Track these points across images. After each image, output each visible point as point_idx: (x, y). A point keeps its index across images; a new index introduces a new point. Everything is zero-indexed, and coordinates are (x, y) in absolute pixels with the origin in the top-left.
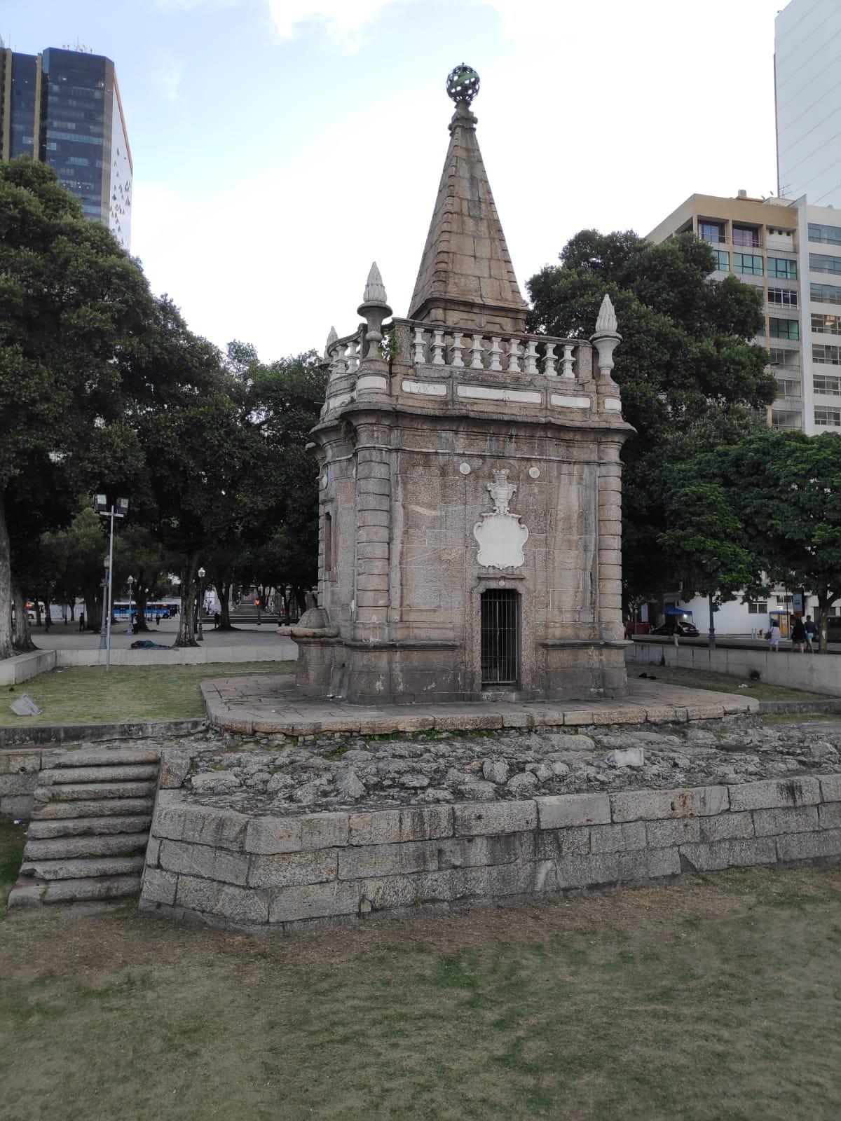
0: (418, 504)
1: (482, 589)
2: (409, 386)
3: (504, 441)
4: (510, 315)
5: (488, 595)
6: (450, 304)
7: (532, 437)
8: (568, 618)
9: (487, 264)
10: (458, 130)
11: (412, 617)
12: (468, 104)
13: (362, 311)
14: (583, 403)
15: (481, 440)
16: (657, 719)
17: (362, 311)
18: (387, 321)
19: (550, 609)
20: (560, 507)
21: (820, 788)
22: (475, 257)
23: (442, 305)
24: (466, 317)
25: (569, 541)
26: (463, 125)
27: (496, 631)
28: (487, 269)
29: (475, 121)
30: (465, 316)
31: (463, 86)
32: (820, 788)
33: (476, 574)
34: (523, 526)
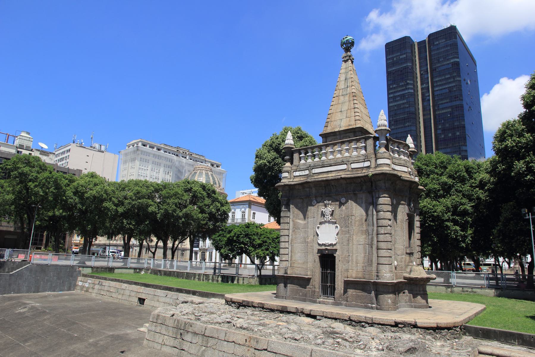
8: (360, 268)
11: (295, 265)
14: (367, 164)
16: (356, 319)
19: (350, 263)
20: (357, 215)
21: (311, 353)
32: (311, 353)
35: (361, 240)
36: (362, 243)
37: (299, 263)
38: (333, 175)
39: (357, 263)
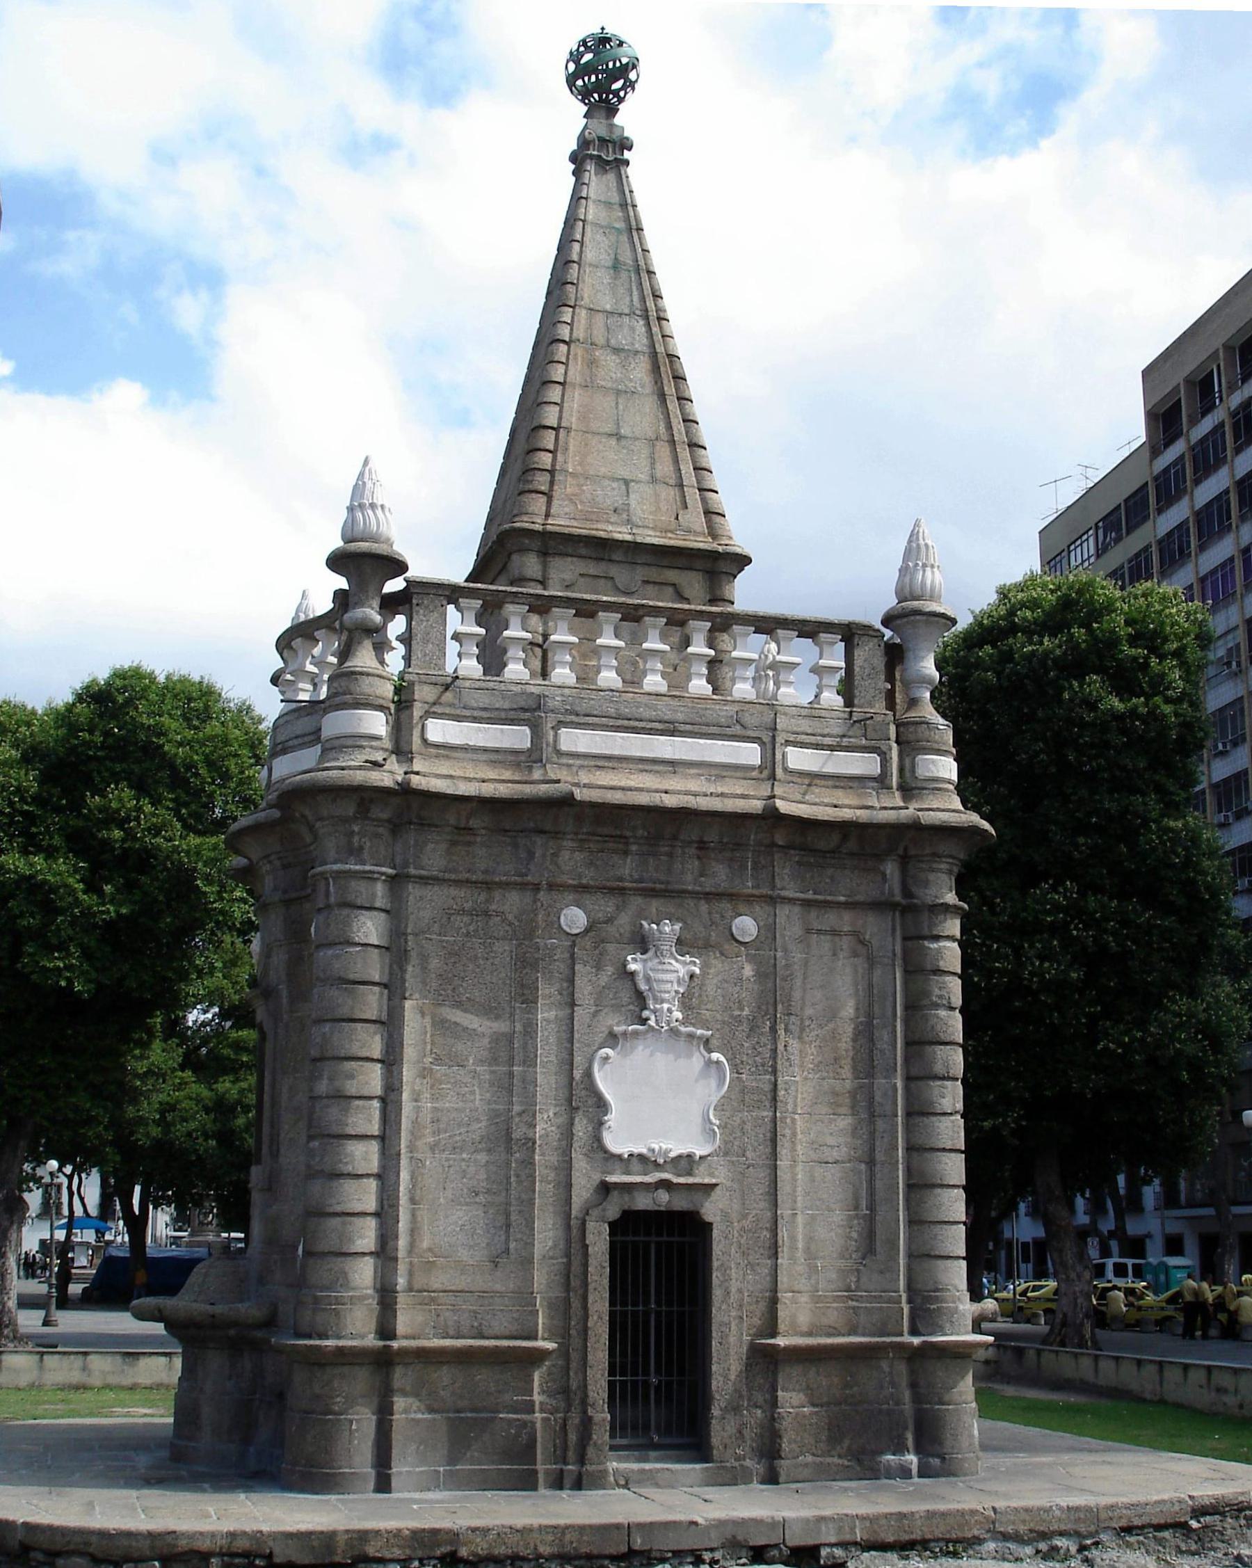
0: (458, 1005)
1: (613, 1210)
2: (438, 731)
3: (670, 855)
4: (699, 564)
5: (630, 1227)
6: (553, 544)
7: (738, 846)
9: (645, 452)
10: (590, 166)
11: (438, 1280)
12: (612, 111)
13: (337, 562)
15: (615, 851)
17: (337, 562)
18: (395, 585)
20: (809, 1011)
22: (619, 437)
23: (537, 544)
24: (592, 571)
25: (835, 1094)
26: (601, 154)
27: (647, 1314)
28: (644, 463)
29: (626, 145)
30: (593, 568)
31: (601, 74)
33: (597, 1177)
34: (716, 1056)
35: (831, 1141)
36: (835, 1155)
37: (462, 1268)
38: (693, 785)
39: (810, 1255)
